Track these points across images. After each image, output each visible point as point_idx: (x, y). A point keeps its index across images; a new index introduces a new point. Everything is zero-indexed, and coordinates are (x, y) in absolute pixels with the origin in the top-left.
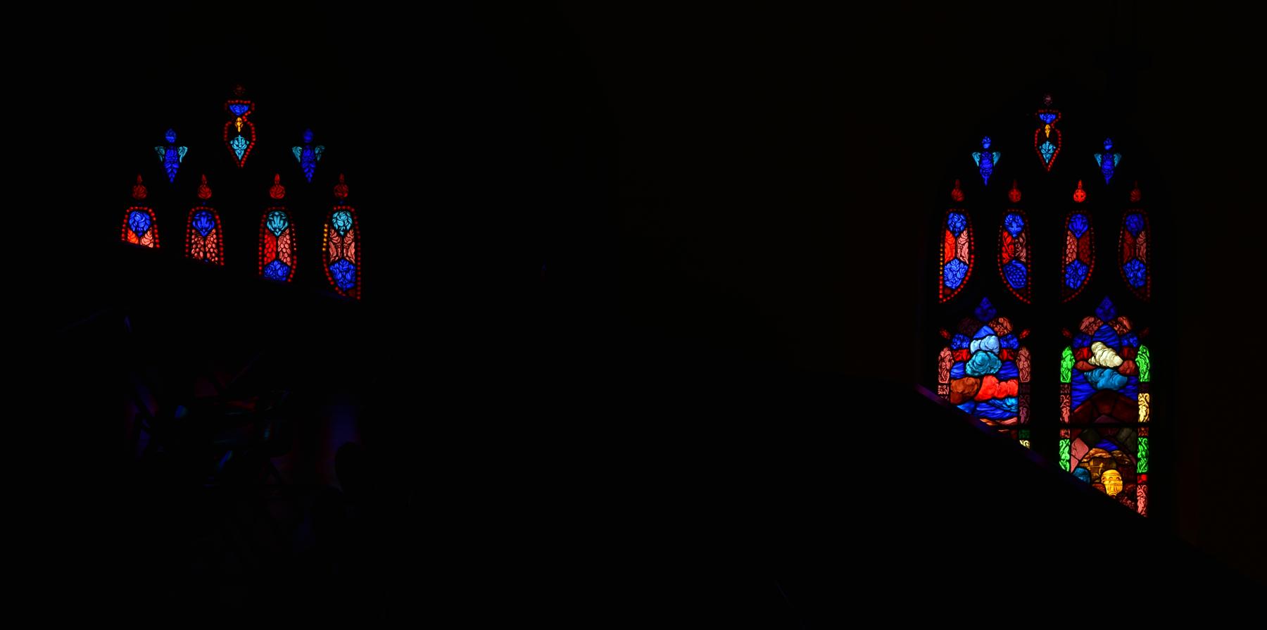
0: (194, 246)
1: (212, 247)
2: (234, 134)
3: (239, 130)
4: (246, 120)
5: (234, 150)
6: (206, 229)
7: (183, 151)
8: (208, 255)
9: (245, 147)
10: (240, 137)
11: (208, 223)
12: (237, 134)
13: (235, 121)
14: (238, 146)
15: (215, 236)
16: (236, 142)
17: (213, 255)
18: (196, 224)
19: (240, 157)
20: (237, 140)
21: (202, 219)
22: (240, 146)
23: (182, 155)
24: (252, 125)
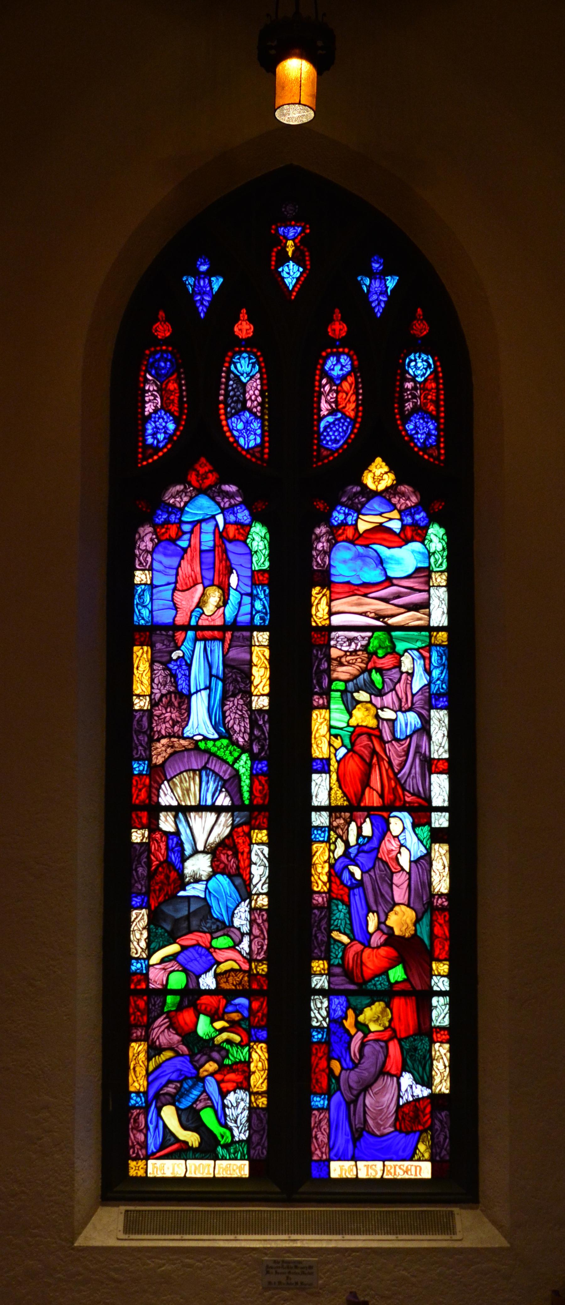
0: (232, 393)
1: (254, 394)
2: (283, 259)
3: (290, 254)
4: (298, 244)
5: (283, 278)
6: (248, 375)
7: (217, 283)
8: (249, 404)
9: (298, 274)
10: (291, 263)
11: (250, 365)
12: (288, 259)
13: (285, 246)
14: (288, 273)
15: (258, 381)
16: (286, 269)
17: (255, 403)
18: (236, 367)
19: (291, 288)
20: (288, 266)
21: (243, 361)
22: (292, 273)
23: (216, 287)
24: (305, 249)
